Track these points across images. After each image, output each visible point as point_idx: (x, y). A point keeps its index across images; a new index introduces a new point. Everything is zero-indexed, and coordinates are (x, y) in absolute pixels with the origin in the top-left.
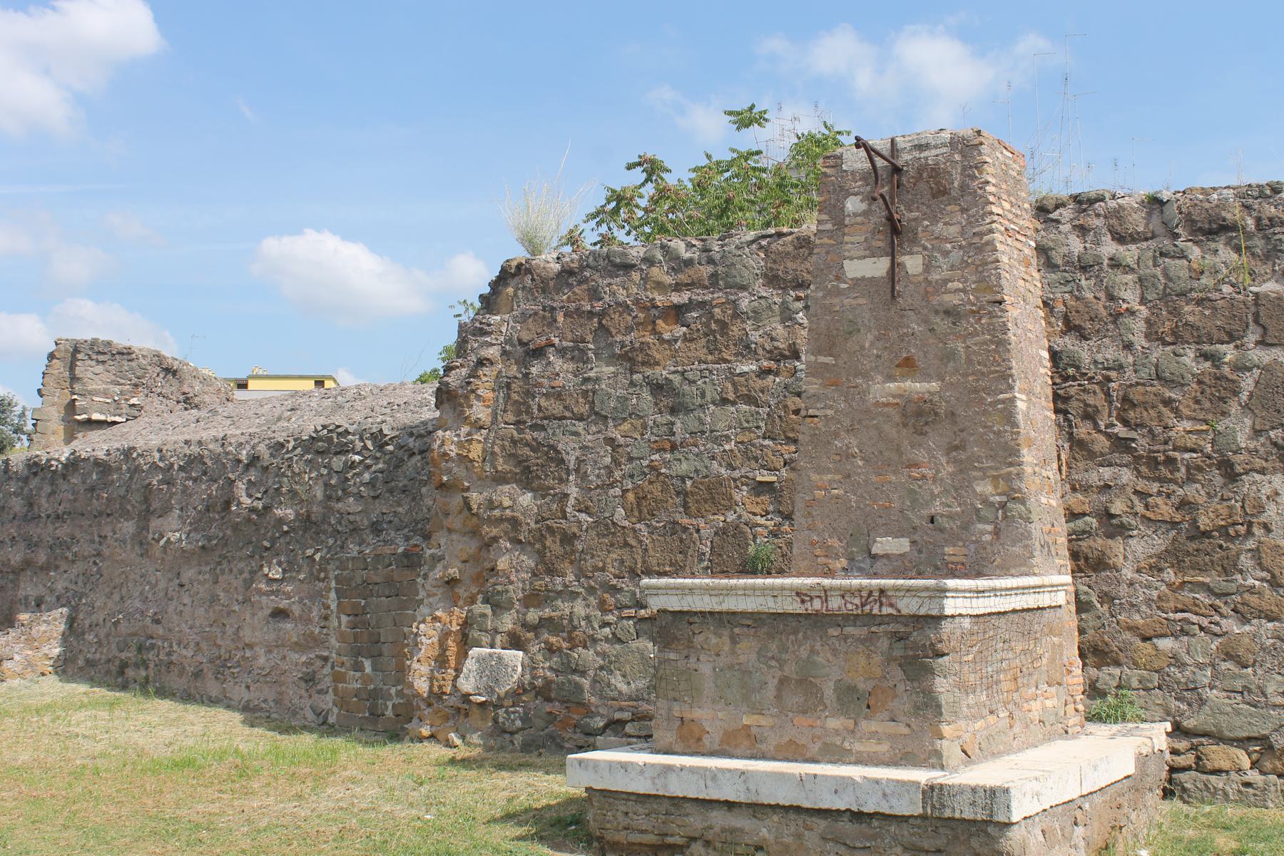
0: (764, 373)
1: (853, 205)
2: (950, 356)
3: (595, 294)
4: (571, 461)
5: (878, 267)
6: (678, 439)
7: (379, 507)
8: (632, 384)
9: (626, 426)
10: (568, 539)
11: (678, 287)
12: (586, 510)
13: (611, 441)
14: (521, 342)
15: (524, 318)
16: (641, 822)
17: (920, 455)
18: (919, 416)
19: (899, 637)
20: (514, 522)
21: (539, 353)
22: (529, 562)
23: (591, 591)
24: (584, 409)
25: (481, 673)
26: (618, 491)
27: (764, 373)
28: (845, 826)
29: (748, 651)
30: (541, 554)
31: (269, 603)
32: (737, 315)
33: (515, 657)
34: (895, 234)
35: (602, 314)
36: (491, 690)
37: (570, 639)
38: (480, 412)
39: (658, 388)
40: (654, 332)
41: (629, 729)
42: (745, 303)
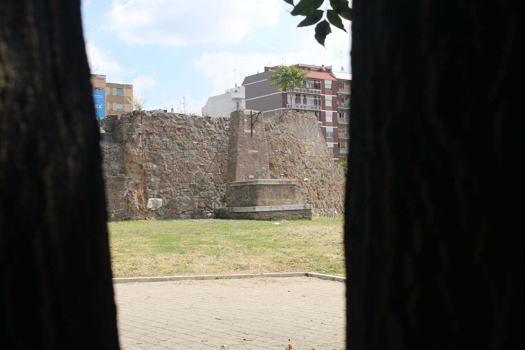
0: (198, 144)
1: (246, 120)
2: (259, 147)
4: (164, 158)
5: (249, 131)
6: (185, 155)
8: (174, 143)
9: (174, 152)
10: (167, 175)
11: (178, 124)
12: (170, 169)
13: (172, 155)
14: (146, 131)
15: (145, 125)
16: (267, 215)
17: (255, 162)
18: (255, 156)
19: (291, 187)
20: (154, 171)
21: (151, 134)
22: (159, 180)
23: (173, 186)
24: (165, 147)
25: (153, 204)
26: (175, 165)
27: (198, 144)
28: (294, 212)
30: (161, 178)
32: (191, 131)
33: (160, 200)
35: (164, 127)
36: (156, 207)
37: (171, 196)
38: (140, 145)
39: (179, 145)
40: (175, 132)
41: (186, 213)
42: (192, 129)
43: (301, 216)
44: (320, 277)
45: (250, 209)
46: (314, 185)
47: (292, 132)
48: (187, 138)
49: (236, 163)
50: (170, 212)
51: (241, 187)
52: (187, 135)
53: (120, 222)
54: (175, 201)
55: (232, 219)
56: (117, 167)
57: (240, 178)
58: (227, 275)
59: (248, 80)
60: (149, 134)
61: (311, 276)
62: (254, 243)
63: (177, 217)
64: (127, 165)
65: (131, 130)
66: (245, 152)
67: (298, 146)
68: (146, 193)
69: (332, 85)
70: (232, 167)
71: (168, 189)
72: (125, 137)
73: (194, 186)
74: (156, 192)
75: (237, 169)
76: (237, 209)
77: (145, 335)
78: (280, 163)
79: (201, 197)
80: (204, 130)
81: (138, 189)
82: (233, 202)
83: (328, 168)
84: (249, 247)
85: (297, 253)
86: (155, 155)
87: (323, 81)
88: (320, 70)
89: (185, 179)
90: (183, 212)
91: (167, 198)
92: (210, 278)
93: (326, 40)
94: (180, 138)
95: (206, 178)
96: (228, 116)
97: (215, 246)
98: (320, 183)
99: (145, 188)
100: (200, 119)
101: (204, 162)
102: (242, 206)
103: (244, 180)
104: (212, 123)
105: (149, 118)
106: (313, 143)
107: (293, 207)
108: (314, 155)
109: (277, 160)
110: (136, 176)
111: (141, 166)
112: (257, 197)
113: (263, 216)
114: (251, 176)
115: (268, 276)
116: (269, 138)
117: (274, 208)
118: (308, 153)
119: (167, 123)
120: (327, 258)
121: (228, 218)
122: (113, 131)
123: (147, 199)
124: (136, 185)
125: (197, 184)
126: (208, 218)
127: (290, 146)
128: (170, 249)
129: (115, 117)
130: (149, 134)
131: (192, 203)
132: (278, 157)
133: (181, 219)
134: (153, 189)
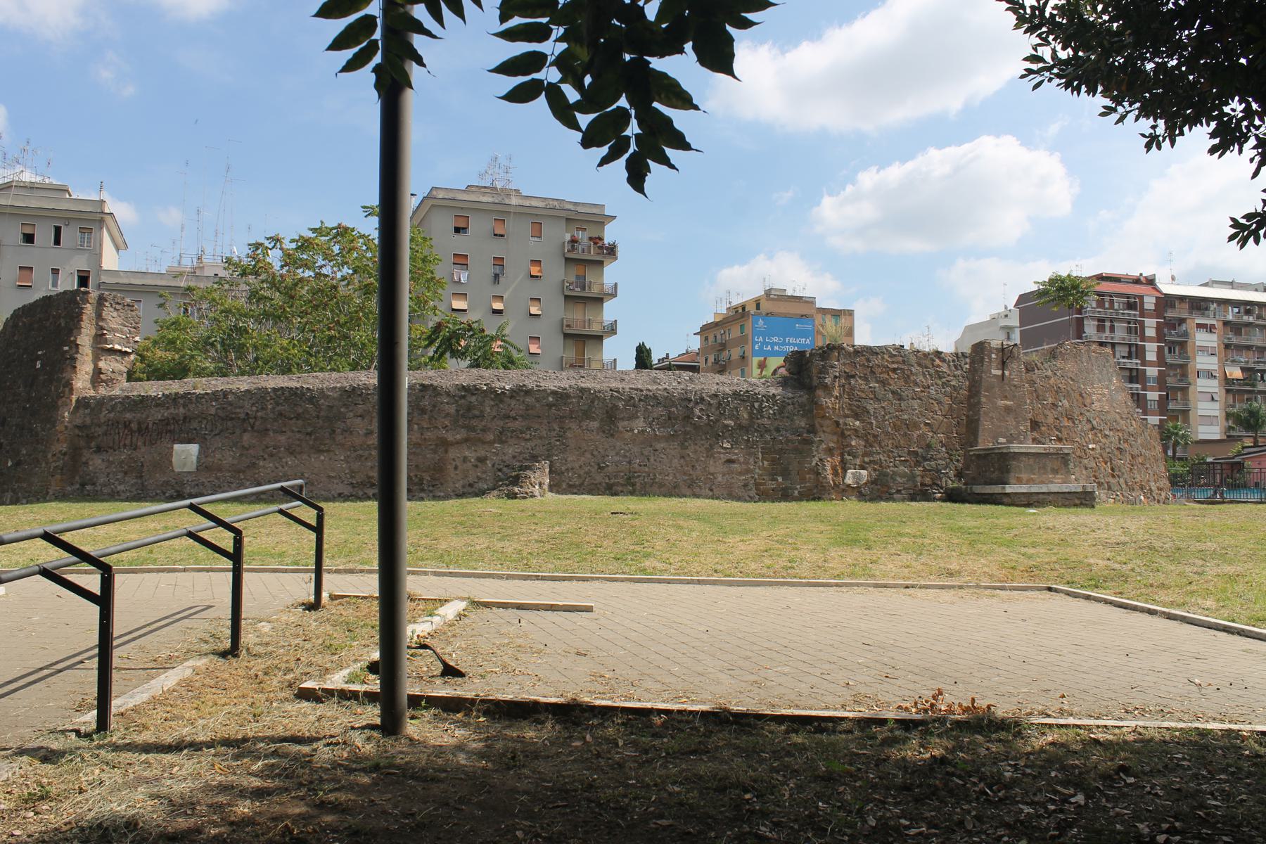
3: (868, 360)
4: (872, 411)
5: (999, 373)
7: (776, 423)
10: (875, 436)
15: (844, 364)
18: (1008, 409)
21: (853, 376)
29: (1031, 462)
30: (867, 441)
31: (724, 457)
33: (864, 472)
34: (1003, 365)
39: (893, 392)
43: (1078, 502)
44: (1068, 594)
45: (997, 489)
46: (1105, 455)
47: (1070, 375)
48: (906, 382)
49: (978, 420)
50: (878, 490)
51: (986, 456)
52: (907, 379)
53: (804, 503)
54: (886, 475)
55: (969, 503)
56: (803, 424)
57: (985, 443)
58: (922, 583)
59: (1023, 299)
60: (849, 377)
61: (1056, 591)
62: (982, 538)
63: (890, 498)
64: (817, 421)
65: (823, 371)
66: (993, 404)
67: (1081, 395)
68: (843, 462)
69: (1156, 305)
70: (971, 428)
71: (877, 457)
72: (815, 382)
73: (916, 453)
74: (858, 461)
75: (981, 428)
76: (978, 489)
77: (747, 658)
78: (1050, 420)
79: (925, 470)
80: (932, 371)
81: (832, 456)
82: (974, 479)
83: (1131, 429)
84: (972, 544)
85: (1042, 555)
86: (858, 407)
87: (1141, 297)
88: (1137, 281)
89: (902, 443)
90: (899, 492)
91: (875, 470)
92: (895, 586)
93: (646, 185)
94: (896, 383)
95: (933, 441)
96: (968, 351)
97: (919, 541)
98: (1116, 452)
99: (842, 455)
100: (926, 355)
101: (931, 417)
102: (986, 483)
103: (990, 446)
104: (944, 361)
105: (849, 354)
106: (1106, 391)
107: (1065, 488)
108: (1106, 408)
109: (1046, 416)
110: (830, 437)
111: (837, 423)
112: (1008, 471)
113: (1016, 500)
114: (1002, 440)
115: (987, 588)
116: (1031, 383)
117: (1035, 489)
118: (1097, 406)
119: (876, 361)
120: (1089, 565)
121: (963, 501)
122: (799, 373)
123: (845, 470)
124: (830, 451)
125: (920, 451)
126: (935, 500)
127: (1067, 396)
128: (853, 542)
129: (802, 354)
130: (849, 377)
131: (912, 477)
132: (1047, 412)
133: (894, 500)
134: (854, 457)
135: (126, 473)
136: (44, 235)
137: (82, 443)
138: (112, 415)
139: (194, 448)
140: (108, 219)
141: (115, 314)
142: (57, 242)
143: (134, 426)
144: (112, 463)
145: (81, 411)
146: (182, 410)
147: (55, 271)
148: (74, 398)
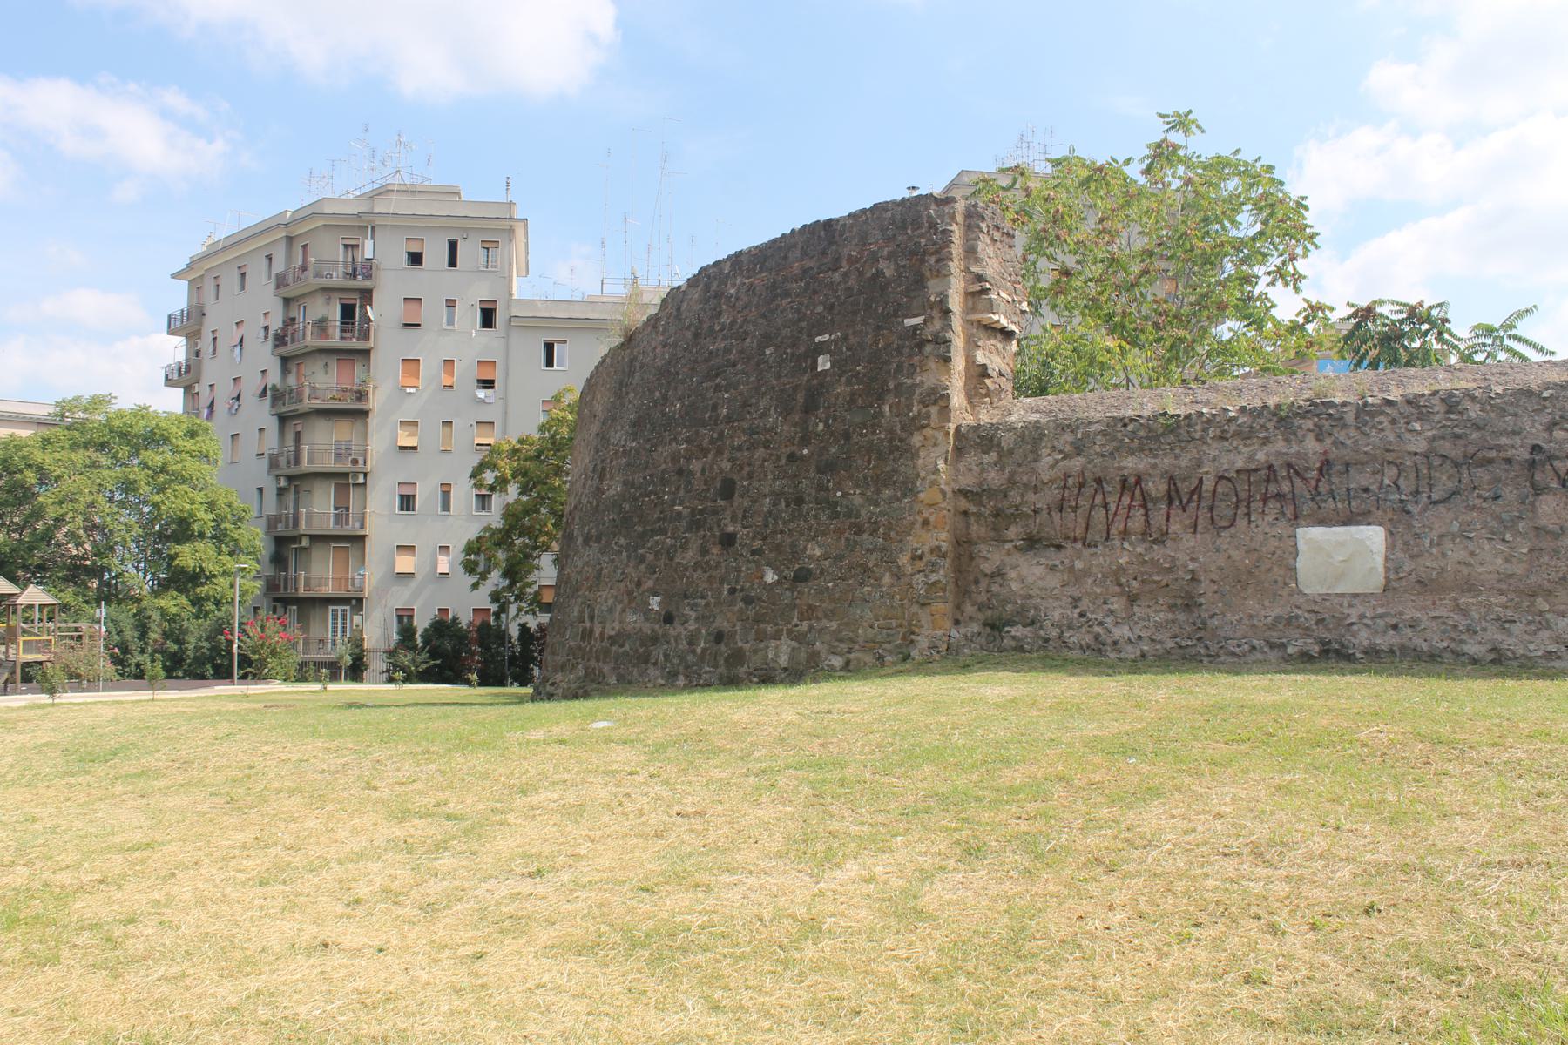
135: (1132, 599)
136: (435, 254)
137: (976, 529)
138: (1077, 463)
139: (1373, 537)
140: (520, 232)
141: (990, 251)
142: (452, 262)
143: (1156, 487)
144: (1086, 573)
145: (971, 458)
146: (1311, 444)
147: (451, 303)
148: (952, 426)
